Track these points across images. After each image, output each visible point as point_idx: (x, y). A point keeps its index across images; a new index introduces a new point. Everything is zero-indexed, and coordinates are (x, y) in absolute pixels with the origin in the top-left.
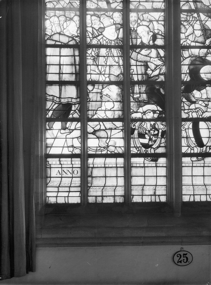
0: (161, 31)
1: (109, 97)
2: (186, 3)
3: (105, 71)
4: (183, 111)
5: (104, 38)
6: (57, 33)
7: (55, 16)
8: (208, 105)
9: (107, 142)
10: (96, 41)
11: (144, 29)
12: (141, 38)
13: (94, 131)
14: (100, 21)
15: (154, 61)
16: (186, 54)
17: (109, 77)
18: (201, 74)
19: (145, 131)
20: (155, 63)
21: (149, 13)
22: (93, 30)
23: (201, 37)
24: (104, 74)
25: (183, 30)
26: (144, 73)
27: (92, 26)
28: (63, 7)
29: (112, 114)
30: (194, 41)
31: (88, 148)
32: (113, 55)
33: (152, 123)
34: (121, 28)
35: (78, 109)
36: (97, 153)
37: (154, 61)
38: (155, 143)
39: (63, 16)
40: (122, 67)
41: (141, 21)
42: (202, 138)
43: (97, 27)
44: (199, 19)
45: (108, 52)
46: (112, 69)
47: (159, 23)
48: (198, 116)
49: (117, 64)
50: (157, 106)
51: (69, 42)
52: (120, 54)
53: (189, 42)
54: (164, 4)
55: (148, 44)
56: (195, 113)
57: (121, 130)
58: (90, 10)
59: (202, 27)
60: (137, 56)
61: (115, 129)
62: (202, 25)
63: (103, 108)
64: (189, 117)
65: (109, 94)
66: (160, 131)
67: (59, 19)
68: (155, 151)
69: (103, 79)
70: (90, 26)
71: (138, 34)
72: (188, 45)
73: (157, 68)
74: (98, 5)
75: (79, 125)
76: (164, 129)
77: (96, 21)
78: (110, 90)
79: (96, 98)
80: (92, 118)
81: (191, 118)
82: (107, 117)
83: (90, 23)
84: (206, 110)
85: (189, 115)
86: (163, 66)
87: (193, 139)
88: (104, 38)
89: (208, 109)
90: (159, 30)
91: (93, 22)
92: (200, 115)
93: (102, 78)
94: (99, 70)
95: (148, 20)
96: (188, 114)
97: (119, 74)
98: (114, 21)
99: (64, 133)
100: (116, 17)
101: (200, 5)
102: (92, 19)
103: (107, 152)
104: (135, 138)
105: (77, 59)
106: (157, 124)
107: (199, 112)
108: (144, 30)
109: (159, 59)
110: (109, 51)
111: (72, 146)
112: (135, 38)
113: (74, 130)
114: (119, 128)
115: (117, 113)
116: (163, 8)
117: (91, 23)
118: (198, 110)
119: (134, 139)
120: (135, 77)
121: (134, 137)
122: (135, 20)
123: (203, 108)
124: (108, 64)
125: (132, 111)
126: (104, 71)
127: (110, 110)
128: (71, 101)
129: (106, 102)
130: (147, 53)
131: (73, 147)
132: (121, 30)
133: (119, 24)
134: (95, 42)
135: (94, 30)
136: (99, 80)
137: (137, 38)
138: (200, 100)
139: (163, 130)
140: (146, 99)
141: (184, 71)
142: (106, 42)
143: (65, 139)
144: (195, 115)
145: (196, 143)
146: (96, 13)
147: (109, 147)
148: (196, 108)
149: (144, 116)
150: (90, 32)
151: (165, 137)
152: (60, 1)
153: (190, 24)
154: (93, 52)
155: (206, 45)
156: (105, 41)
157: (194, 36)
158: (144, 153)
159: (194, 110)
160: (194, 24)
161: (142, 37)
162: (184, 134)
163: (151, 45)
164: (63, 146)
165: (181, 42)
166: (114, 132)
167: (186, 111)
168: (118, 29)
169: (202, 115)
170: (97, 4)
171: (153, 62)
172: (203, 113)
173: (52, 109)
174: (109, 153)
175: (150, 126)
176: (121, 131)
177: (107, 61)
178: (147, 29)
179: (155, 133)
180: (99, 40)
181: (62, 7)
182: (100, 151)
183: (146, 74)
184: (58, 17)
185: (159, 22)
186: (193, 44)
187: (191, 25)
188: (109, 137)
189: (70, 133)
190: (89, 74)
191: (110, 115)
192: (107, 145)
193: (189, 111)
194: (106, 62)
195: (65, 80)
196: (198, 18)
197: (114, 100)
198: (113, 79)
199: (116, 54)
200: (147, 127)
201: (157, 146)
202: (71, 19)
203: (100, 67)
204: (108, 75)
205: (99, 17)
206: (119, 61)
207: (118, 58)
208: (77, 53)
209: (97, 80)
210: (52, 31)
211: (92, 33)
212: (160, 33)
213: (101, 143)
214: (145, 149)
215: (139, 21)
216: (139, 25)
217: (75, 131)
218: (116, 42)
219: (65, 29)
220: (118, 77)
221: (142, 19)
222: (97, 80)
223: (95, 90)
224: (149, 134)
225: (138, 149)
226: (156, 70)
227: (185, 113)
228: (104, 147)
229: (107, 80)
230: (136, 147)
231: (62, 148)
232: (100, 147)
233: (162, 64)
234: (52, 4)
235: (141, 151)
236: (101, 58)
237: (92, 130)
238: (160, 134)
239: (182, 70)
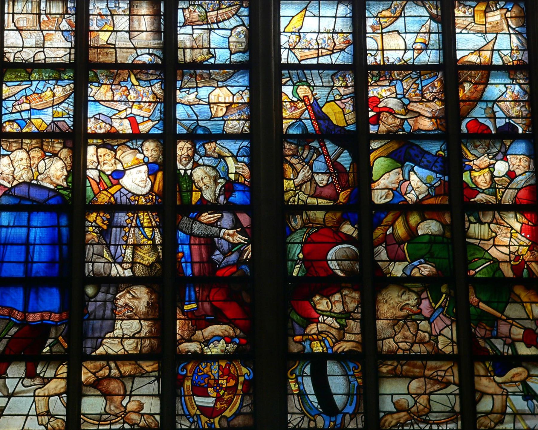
0: (244, 177)
1: (130, 311)
2: (297, 121)
3: (123, 255)
4: (290, 338)
5: (122, 190)
6: (24, 182)
7: (21, 148)
8: (346, 326)
9: (124, 403)
10: (105, 197)
11: (206, 173)
12: (200, 189)
13: (95, 381)
14: (115, 158)
15: (229, 235)
16: (297, 222)
17: (131, 268)
18: (329, 262)
19: (206, 380)
20: (231, 239)
21: (218, 142)
22: (100, 176)
23: (328, 186)
24: (120, 264)
25: (290, 173)
26: (205, 260)
27: (99, 168)
28: (38, 130)
29: (137, 346)
30: (316, 194)
31: (82, 416)
32: (141, 223)
33: (223, 364)
34: (159, 170)
35: (63, 334)
36: (101, 428)
37: (229, 235)
38: (229, 406)
39: (37, 149)
40: (159, 248)
41: (201, 157)
42: (334, 396)
43: (108, 169)
44: (323, 152)
45: (132, 218)
46: (140, 253)
47: (238, 161)
48: (325, 349)
49: (150, 242)
50: (233, 328)
51: (49, 198)
52: (156, 222)
53: (303, 197)
54: (247, 124)
55: (216, 202)
56: (318, 342)
57: (153, 379)
58: (95, 136)
59: (330, 167)
60: (192, 225)
61: (142, 376)
62: (329, 163)
63: (118, 332)
64: (304, 350)
65: (131, 304)
66: (241, 379)
67: (29, 155)
68: (228, 423)
69: (118, 273)
70: (94, 167)
71: (193, 182)
72: (301, 203)
73: (233, 250)
74: (111, 126)
75: (63, 370)
76: (249, 376)
77: (107, 158)
78: (133, 296)
79: (102, 311)
80: (94, 354)
81: (308, 354)
82: (125, 350)
83: (94, 161)
84: (342, 336)
85: (304, 347)
86: (248, 245)
87: (313, 398)
88: (122, 190)
89: (346, 334)
90: (240, 174)
91: (101, 159)
92: (328, 346)
93: (116, 271)
94: (111, 253)
95: (216, 155)
96: (302, 344)
97: (153, 263)
98: (145, 156)
99: (31, 386)
100: (150, 149)
101: (327, 125)
102: (99, 154)
103: (123, 426)
104: (185, 396)
105: (64, 231)
106: (234, 365)
107: (326, 341)
109: (237, 232)
110: (134, 217)
111: (48, 413)
112: (187, 191)
113: (52, 378)
114: (151, 374)
115: (148, 342)
116: (246, 131)
117: (96, 161)
118: (326, 336)
119: (183, 398)
120: (186, 268)
121: (183, 394)
122: (188, 155)
123: (334, 332)
124: (130, 241)
125: (178, 337)
126: (121, 255)
127: (133, 337)
128: (50, 318)
129: (124, 322)
130: (212, 219)
131: (47, 415)
132: (160, 175)
133: (155, 163)
134: (103, 198)
135: (102, 174)
136: (110, 273)
137: (191, 191)
138: (328, 316)
139: (246, 377)
140: (210, 314)
141: (292, 255)
142: (127, 198)
143: (33, 398)
144: (317, 347)
145: (319, 407)
146: (108, 141)
147: (127, 414)
148: (320, 333)
149: (206, 348)
150: (93, 179)
151: (251, 392)
152: (32, 120)
153: (306, 160)
154: (99, 218)
155: (340, 202)
156: (125, 197)
157: (314, 185)
158: (206, 427)
159: (315, 337)
160: (313, 161)
161: (204, 187)
162: (294, 387)
163: (222, 203)
164: (26, 413)
165: (286, 197)
166: (138, 382)
167: (298, 338)
168: (152, 173)
169: (334, 346)
170: (111, 123)
171: (226, 237)
172: (334, 343)
173: (6, 336)
174: (127, 426)
175: (219, 369)
176: (154, 381)
177: (128, 237)
178: (213, 173)
179: (229, 385)
180: (113, 195)
181: (36, 131)
182: (109, 422)
183: (210, 261)
184: (28, 152)
185: (239, 159)
186: (312, 201)
187: (307, 163)
188: (128, 393)
189: (44, 385)
190: (89, 262)
191: (130, 346)
192: (123, 410)
193: (305, 338)
194: (125, 238)
195: (38, 275)
196: (322, 149)
197: (142, 317)
198: (140, 271)
199: (149, 222)
200: (211, 372)
201: (234, 411)
202: (55, 155)
203: (112, 248)
204: (130, 265)
205: (111, 148)
206: (154, 237)
207: (151, 229)
208: (64, 221)
209: (106, 275)
210: (14, 178)
211: (98, 181)
212: (241, 180)
213: (110, 405)
214: (208, 419)
215: (197, 157)
216: (196, 165)
217: (55, 380)
218: (149, 199)
219: (42, 174)
220: (151, 269)
221: (202, 152)
222: (105, 274)
223: (101, 296)
224: (217, 386)
225: (191, 420)
226: (233, 253)
227: (296, 342)
228: (116, 415)
229: (128, 273)
230: (188, 416)
231: (25, 417)
232: (107, 413)
233: (245, 240)
234: (16, 125)
235: (198, 423)
236: (116, 231)
237: (92, 380)
238: (240, 387)
239: (288, 252)
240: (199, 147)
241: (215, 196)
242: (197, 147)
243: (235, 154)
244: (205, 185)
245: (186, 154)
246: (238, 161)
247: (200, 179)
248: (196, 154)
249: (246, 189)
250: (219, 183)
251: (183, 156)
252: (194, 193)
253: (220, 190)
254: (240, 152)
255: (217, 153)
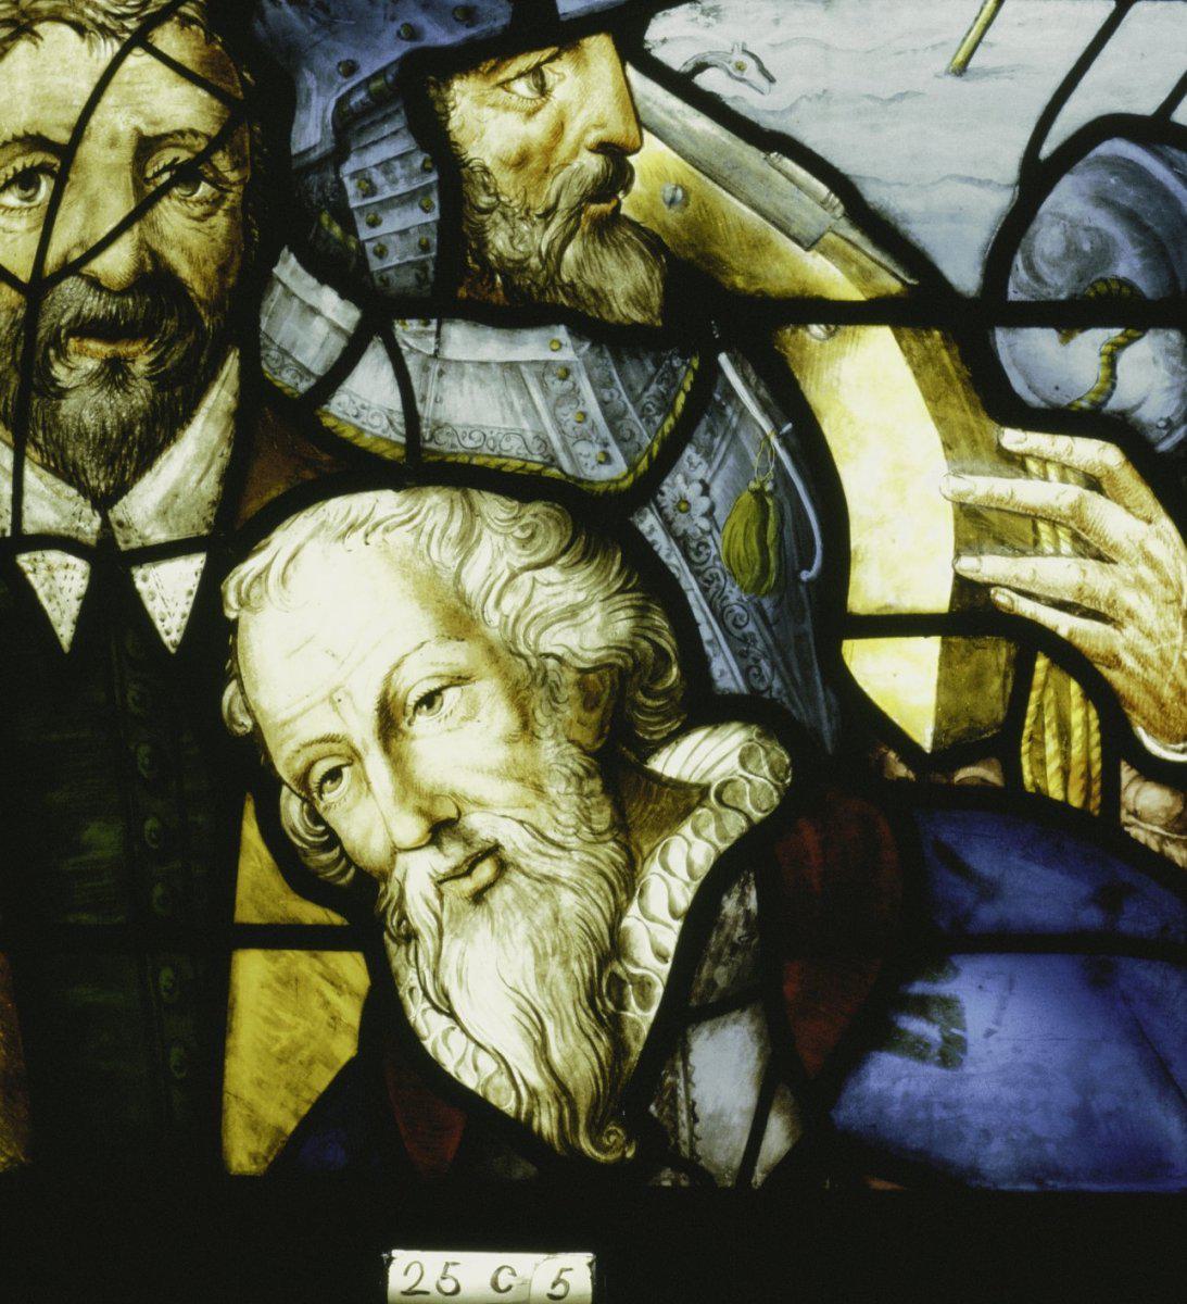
11: (459, 620)
90: (1030, 639)
108: (457, 656)
122: (154, 278)
240: (349, 128)
241: (612, 1025)
242: (311, 131)
243: (964, 273)
244: (440, 830)
245: (117, 263)
246: (1002, 404)
247: (361, 728)
248: (289, 269)
249: (1135, 920)
250: (685, 799)
251: (73, 297)
252: (252, 970)
253: (700, 919)
254: (1047, 238)
255: (653, 244)
